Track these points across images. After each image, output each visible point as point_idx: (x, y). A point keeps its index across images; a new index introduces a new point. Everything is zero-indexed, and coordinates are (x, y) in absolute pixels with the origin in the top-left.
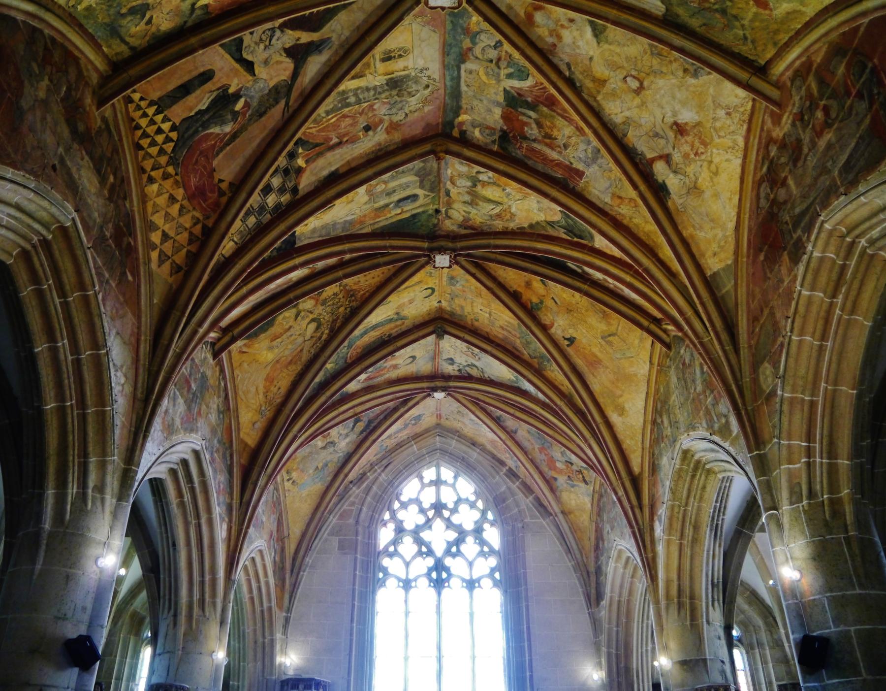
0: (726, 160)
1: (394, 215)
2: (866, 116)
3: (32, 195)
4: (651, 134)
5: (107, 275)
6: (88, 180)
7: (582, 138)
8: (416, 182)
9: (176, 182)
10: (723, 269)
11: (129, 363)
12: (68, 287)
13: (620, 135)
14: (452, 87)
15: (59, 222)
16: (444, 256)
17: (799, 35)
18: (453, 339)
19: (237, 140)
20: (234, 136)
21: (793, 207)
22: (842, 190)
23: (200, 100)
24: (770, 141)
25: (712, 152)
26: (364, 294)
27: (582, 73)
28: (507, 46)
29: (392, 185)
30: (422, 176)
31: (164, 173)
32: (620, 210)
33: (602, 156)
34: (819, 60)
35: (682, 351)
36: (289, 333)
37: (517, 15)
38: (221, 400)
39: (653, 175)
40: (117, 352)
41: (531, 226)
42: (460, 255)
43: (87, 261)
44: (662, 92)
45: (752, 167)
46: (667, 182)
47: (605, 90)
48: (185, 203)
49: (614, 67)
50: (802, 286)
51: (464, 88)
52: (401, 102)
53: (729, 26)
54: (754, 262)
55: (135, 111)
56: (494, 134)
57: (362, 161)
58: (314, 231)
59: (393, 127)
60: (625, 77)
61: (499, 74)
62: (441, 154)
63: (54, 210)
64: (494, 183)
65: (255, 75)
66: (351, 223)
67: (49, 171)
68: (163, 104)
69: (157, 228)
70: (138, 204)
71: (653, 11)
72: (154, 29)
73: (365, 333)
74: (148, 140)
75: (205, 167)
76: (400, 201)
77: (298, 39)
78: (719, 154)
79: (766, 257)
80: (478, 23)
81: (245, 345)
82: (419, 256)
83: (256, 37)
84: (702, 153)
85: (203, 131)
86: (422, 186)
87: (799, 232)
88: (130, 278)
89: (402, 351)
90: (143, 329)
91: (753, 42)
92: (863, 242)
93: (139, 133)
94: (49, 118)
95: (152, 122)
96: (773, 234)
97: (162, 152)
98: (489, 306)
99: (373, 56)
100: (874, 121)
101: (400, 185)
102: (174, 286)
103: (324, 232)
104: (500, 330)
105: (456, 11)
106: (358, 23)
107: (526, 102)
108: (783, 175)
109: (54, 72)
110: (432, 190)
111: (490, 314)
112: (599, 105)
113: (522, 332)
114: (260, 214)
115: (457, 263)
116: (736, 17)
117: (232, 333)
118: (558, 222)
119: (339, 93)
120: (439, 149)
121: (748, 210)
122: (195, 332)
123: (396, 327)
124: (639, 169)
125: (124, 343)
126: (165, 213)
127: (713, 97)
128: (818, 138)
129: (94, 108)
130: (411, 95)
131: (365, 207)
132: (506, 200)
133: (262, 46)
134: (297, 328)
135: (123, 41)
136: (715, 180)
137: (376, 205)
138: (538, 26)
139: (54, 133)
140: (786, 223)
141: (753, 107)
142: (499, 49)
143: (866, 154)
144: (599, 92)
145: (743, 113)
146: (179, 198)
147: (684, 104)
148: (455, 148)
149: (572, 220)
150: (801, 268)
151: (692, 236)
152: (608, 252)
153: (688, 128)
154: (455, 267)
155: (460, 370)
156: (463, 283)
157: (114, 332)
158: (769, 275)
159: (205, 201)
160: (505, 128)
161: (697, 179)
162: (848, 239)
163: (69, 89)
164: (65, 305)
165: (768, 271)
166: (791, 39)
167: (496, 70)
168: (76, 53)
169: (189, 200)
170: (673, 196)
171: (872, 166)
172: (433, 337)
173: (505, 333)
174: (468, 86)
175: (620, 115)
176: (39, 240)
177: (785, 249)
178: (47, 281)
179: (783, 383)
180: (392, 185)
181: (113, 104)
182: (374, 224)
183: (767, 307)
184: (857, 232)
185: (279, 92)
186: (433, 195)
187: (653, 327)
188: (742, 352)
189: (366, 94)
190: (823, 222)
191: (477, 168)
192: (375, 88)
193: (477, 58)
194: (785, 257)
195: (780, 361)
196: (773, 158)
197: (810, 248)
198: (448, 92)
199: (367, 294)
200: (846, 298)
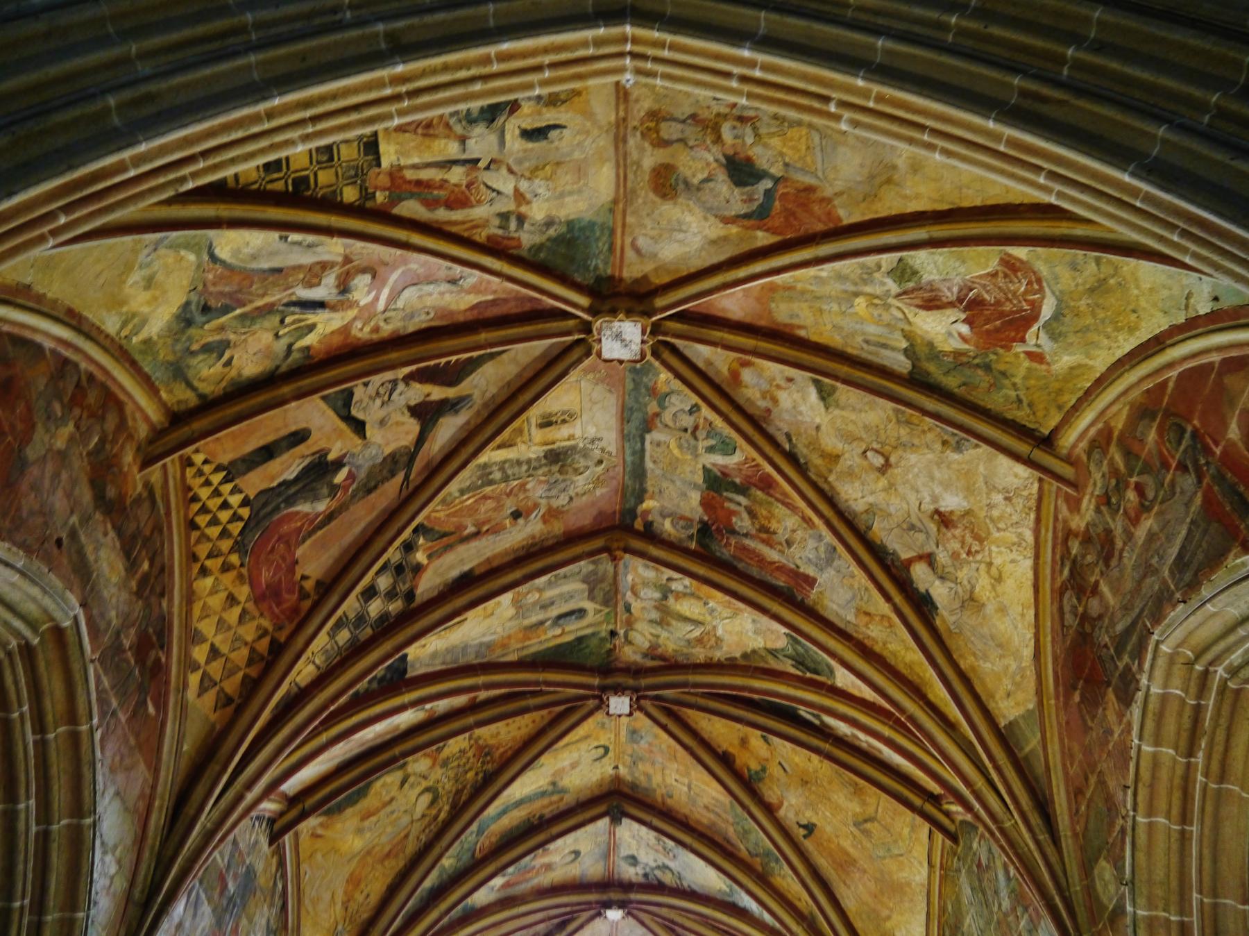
0: (1013, 561)
1: (552, 637)
2: (1196, 493)
3: (16, 578)
4: (905, 526)
5: (114, 703)
6: (108, 562)
7: (811, 532)
8: (583, 591)
9: (240, 577)
10: (1023, 716)
11: (129, 842)
12: (50, 718)
13: (862, 528)
14: (633, 463)
15: (52, 619)
16: (623, 698)
17: (1088, 395)
18: (636, 825)
19: (333, 524)
20: (330, 517)
21: (1113, 624)
22: (1178, 595)
23: (288, 467)
24: (1069, 534)
25: (990, 550)
26: (505, 752)
27: (807, 447)
28: (706, 411)
29: (550, 594)
30: (592, 582)
31: (224, 563)
32: (869, 632)
33: (840, 557)
34: (1120, 426)
35: (975, 845)
36: (389, 809)
37: (718, 372)
38: (274, 911)
39: (912, 582)
40: (112, 823)
41: (745, 656)
42: (645, 697)
43: (87, 680)
44: (916, 470)
45: (1048, 571)
46: (932, 592)
47: (838, 468)
48: (250, 606)
49: (851, 438)
50: (1140, 739)
51: (649, 464)
52: (564, 480)
53: (995, 386)
54: (1066, 704)
55: (194, 476)
56: (691, 527)
57: (506, 559)
58: (434, 655)
59: (552, 514)
60: (865, 452)
61: (696, 448)
62: (619, 553)
63: (47, 602)
64: (692, 595)
65: (364, 437)
66: (489, 646)
67: (50, 546)
68: (232, 472)
69: (204, 640)
70: (181, 603)
71: (896, 367)
72: (233, 373)
73: (504, 812)
74: (208, 517)
75: (284, 559)
76: (560, 617)
77: (428, 395)
78: (1000, 553)
79: (1082, 696)
80: (667, 382)
81: (322, 825)
82: (585, 698)
83: (371, 390)
84: (977, 552)
85: (286, 508)
86: (591, 597)
87: (1126, 659)
88: (151, 710)
89: (560, 842)
90: (159, 789)
91: (1030, 405)
92: (1220, 671)
93: (196, 507)
94: (64, 476)
95: (216, 493)
96: (1090, 664)
97: (225, 534)
98: (687, 774)
99: (528, 419)
100: (1208, 501)
101: (561, 595)
102: (218, 727)
103: (448, 658)
104: (705, 812)
105: (638, 366)
106: (508, 378)
107: (734, 484)
108: (1093, 579)
109: (85, 416)
110: (606, 603)
111: (689, 787)
112: (832, 488)
113: (736, 815)
114: (357, 626)
115: (640, 709)
116: (1004, 374)
117: (301, 805)
118: (783, 650)
119: (479, 466)
120: (615, 545)
121: (1049, 630)
122: (239, 798)
123: (551, 804)
124: (892, 573)
125: (126, 809)
126: (218, 619)
127: (985, 477)
128: (1134, 526)
129: (135, 469)
130: (578, 472)
131: (508, 624)
132: (709, 618)
133: (378, 402)
134: (403, 801)
135: (189, 385)
136: (999, 589)
137: (527, 622)
138: (746, 387)
139: (68, 495)
140: (1106, 646)
141: (1040, 489)
142: (696, 415)
143: (1204, 545)
144: (830, 471)
145: (1028, 498)
146: (242, 598)
147: (947, 486)
148: (637, 544)
149: (803, 646)
150: (1136, 711)
151: (973, 668)
152: (856, 693)
153: (955, 518)
154: (638, 714)
155: (646, 875)
156: (649, 738)
157: (111, 791)
158: (1090, 723)
159: (278, 605)
160: (706, 518)
161: (973, 587)
162: (1198, 668)
163: (103, 440)
164: (42, 745)
165: (1087, 717)
166: (1080, 401)
167: (693, 442)
168: (122, 397)
169: (256, 602)
170: (942, 611)
171: (1215, 559)
172: (606, 820)
173: (712, 816)
174: (655, 462)
175: (861, 502)
176: (19, 646)
177: (1108, 684)
178: (20, 706)
179: (1133, 892)
180: (550, 594)
181: (164, 466)
182: (523, 648)
183: (1092, 772)
184: (1209, 656)
185: (395, 462)
186: (607, 610)
187: (929, 808)
188: (1064, 845)
189: (516, 470)
190: (1158, 643)
191: (669, 573)
192: (529, 462)
193: (666, 426)
194: (1111, 695)
195: (1123, 858)
196: (1076, 556)
197: (1144, 681)
198: (628, 469)
199: (510, 753)
200: (1209, 757)
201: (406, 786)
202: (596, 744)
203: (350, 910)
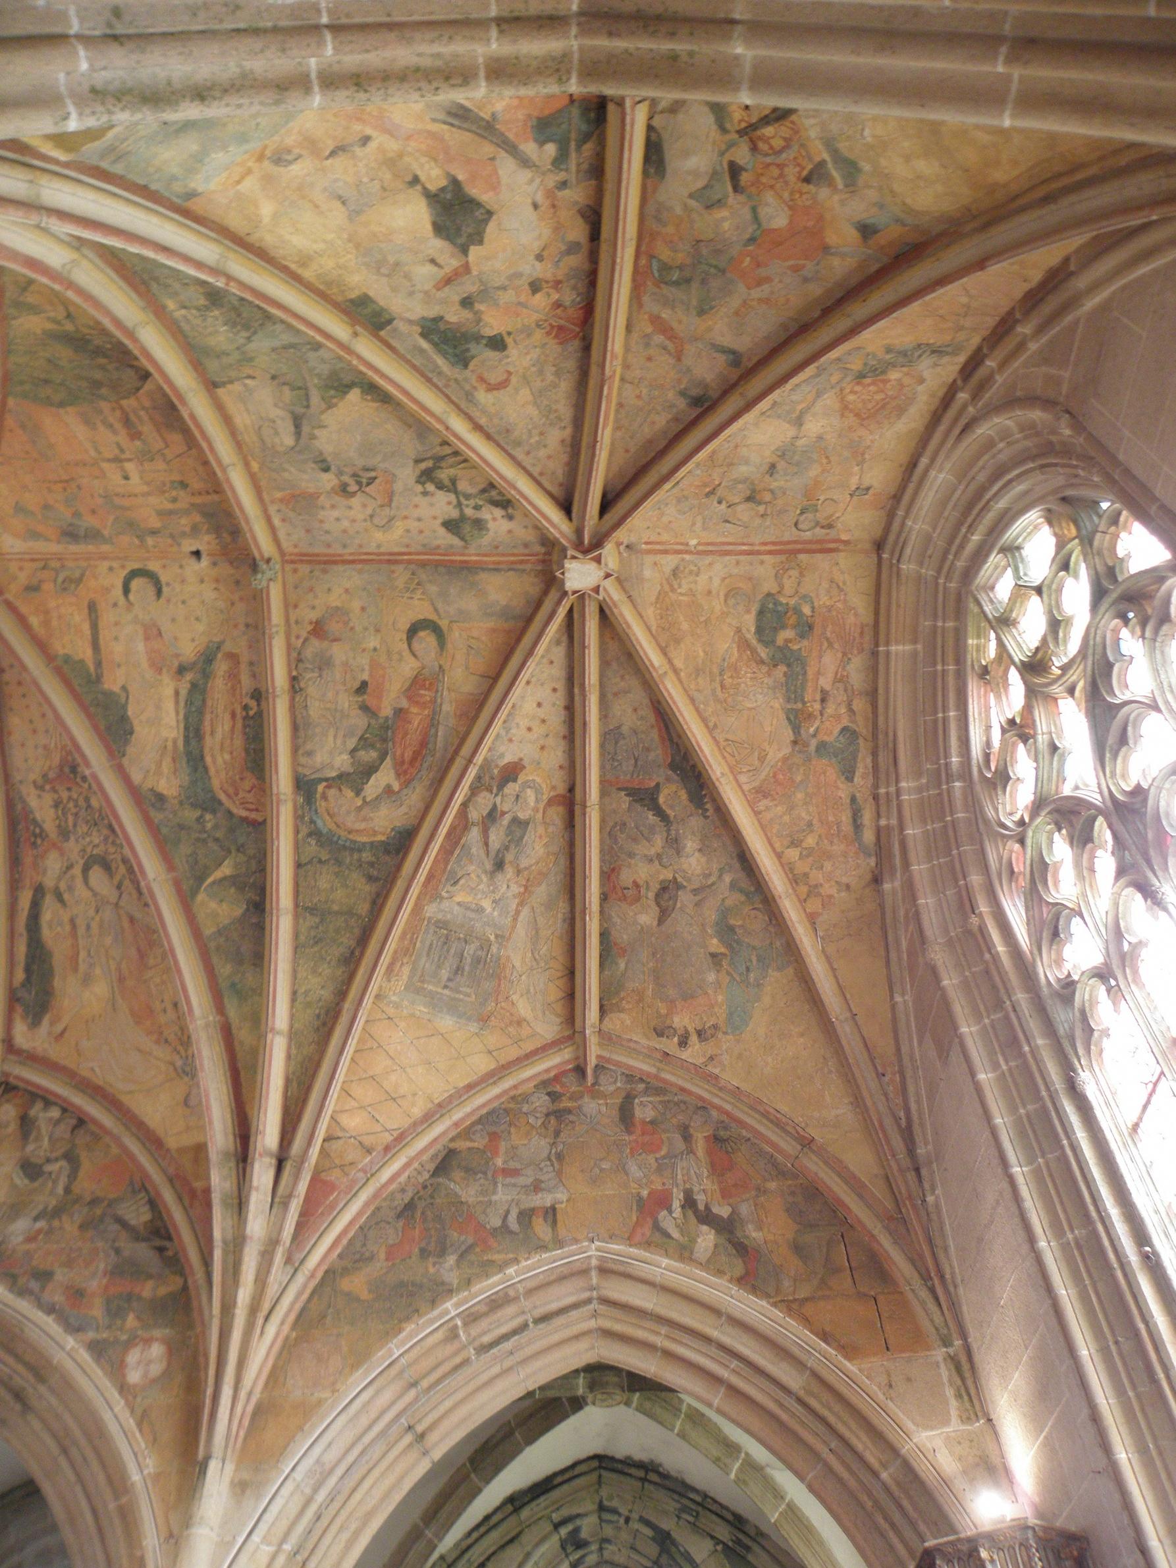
36: (81, 931)
81: (52, 1024)
201: (66, 896)
202: (118, 591)
203: (172, 1038)
